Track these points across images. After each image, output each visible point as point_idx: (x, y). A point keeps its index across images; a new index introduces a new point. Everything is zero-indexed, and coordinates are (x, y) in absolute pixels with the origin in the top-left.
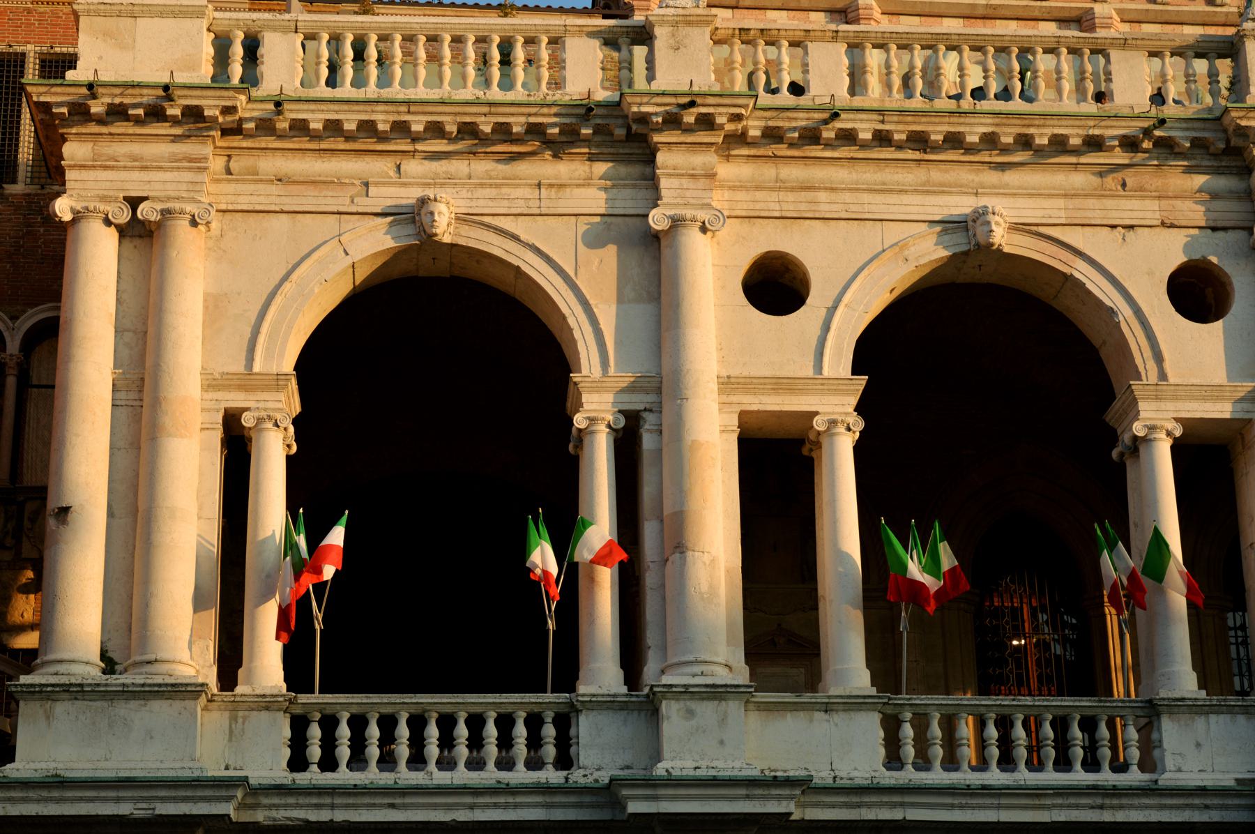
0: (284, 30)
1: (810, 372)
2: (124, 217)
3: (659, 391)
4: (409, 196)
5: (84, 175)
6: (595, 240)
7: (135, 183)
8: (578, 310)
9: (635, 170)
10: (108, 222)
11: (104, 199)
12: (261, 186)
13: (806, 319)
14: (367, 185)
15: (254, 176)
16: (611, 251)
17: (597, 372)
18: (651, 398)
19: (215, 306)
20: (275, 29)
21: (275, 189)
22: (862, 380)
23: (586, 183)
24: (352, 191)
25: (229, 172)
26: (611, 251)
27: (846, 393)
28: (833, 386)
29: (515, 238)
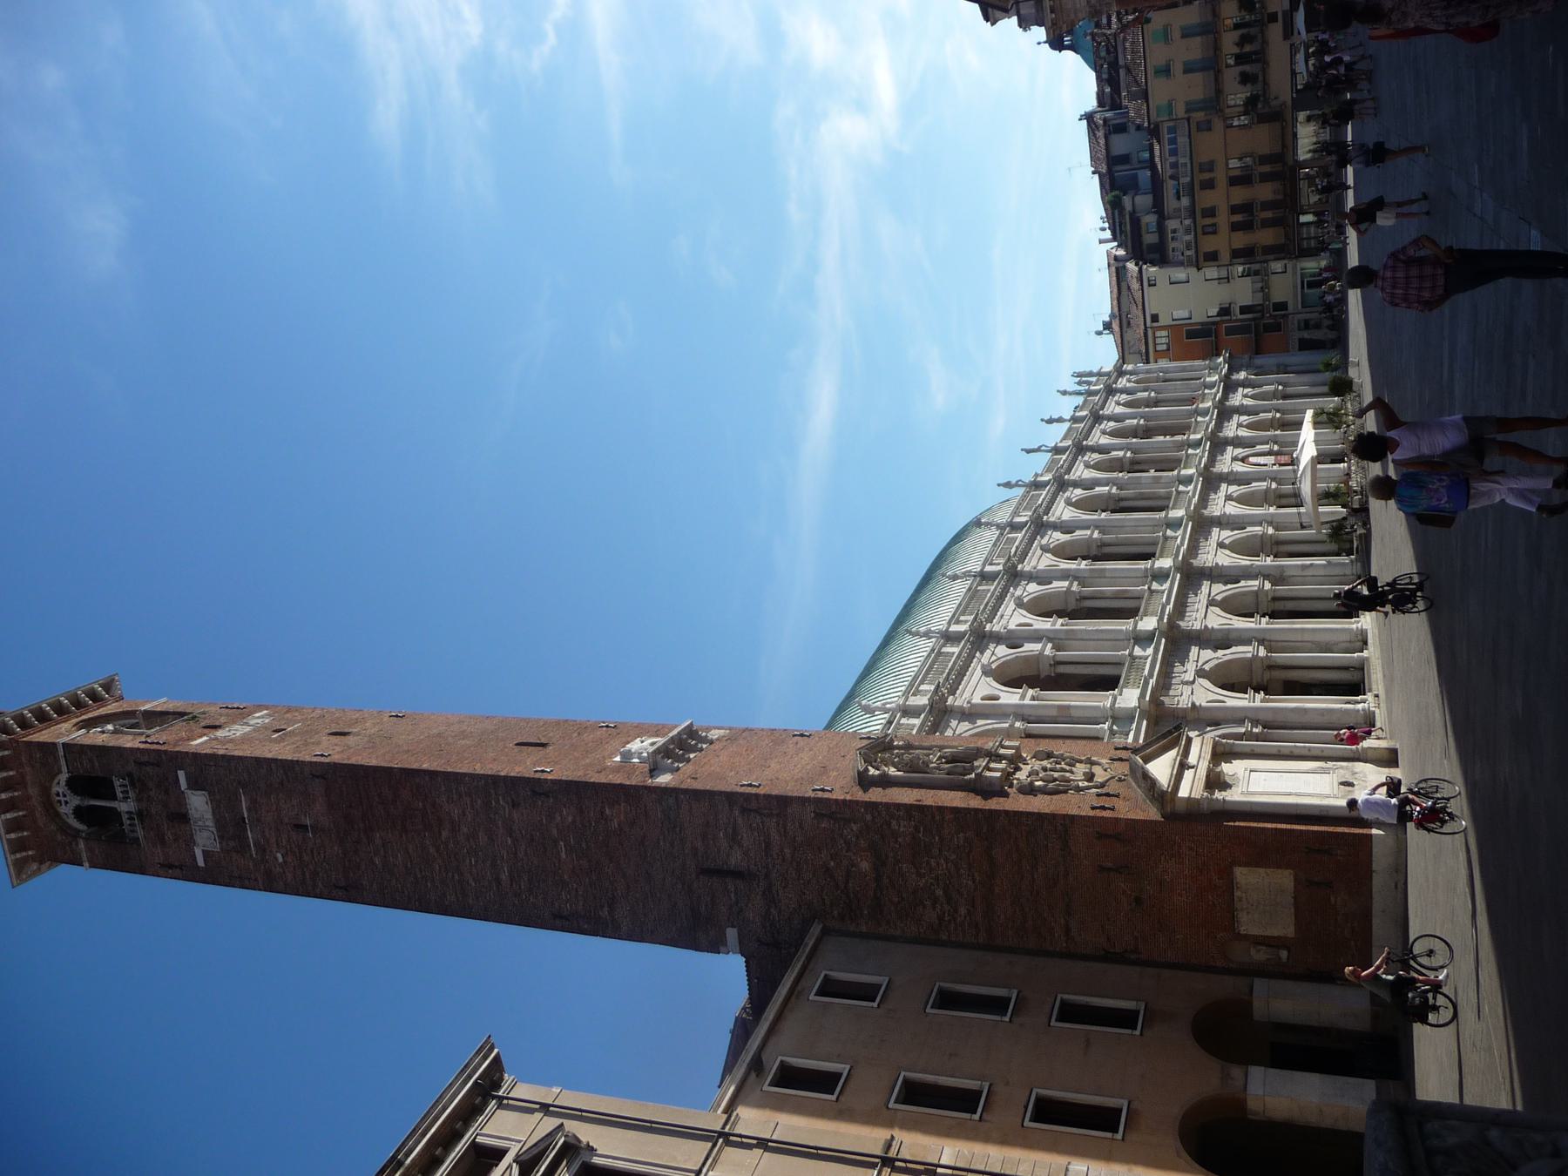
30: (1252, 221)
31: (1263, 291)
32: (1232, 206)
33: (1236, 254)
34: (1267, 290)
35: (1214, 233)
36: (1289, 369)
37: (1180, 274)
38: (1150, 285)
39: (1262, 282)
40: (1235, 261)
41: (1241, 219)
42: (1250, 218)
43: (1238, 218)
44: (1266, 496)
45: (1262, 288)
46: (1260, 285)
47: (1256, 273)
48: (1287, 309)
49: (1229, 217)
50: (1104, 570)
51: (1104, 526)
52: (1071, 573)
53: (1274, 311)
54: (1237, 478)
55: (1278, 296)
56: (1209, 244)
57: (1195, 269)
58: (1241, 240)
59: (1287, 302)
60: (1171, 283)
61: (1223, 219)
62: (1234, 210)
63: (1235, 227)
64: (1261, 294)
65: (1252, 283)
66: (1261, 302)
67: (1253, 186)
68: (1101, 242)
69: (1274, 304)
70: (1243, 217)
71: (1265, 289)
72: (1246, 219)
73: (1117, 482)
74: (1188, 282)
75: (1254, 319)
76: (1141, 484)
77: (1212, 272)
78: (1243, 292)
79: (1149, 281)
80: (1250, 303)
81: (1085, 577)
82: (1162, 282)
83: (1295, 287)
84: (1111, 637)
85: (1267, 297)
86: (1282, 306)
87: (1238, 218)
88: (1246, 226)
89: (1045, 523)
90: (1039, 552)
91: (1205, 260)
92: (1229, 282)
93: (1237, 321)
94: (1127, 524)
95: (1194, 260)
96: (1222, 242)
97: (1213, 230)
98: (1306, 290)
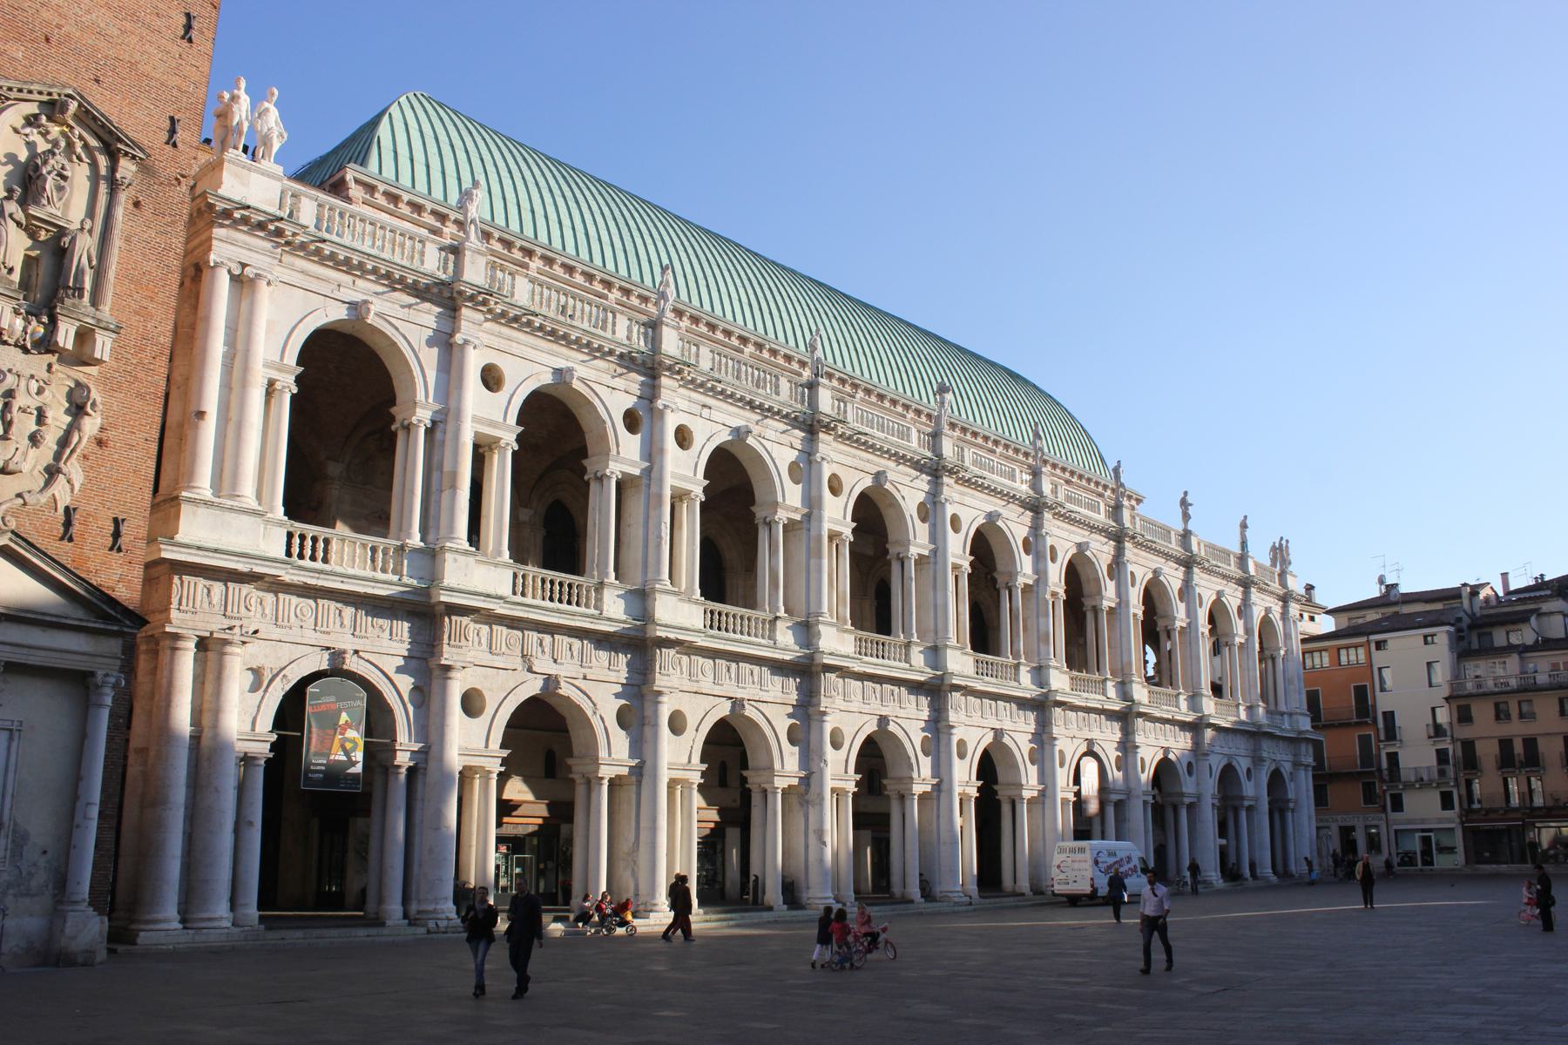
0: (311, 198)
1: (501, 420)
2: (237, 272)
3: (446, 415)
4: (358, 297)
5: (221, 244)
6: (430, 343)
7: (245, 256)
8: (418, 369)
9: (448, 312)
10: (229, 271)
11: (229, 259)
12: (293, 272)
13: (502, 396)
14: (339, 286)
15: (291, 268)
16: (436, 350)
17: (423, 399)
18: (443, 417)
19: (270, 323)
20: (306, 196)
21: (300, 276)
22: (521, 429)
23: (428, 312)
24: (333, 287)
25: (280, 261)
26: (436, 350)
27: (513, 432)
28: (508, 428)
29: (397, 329)
30: (1514, 766)
31: (1417, 781)
32: (1535, 739)
33: (1468, 746)
34: (1417, 786)
35: (1498, 718)
36: (1277, 817)
37: (1442, 674)
38: (1425, 637)
39: (1429, 780)
40: (1459, 745)
41: (1516, 752)
42: (1517, 764)
43: (1518, 748)
44: (1013, 785)
45: (1422, 779)
46: (1425, 778)
47: (1442, 773)
48: (1394, 810)
49: (1518, 736)
50: (819, 556)
51: (935, 563)
52: (815, 512)
53: (1391, 795)
54: (1046, 746)
55: (1409, 799)
56: (1483, 713)
57: (1447, 695)
58: (1488, 752)
59: (1402, 811)
60: (1429, 664)
61: (1516, 729)
62: (1530, 743)
63: (1505, 744)
64: (1413, 779)
65: (1428, 768)
66: (1403, 779)
67: (1563, 767)
68: (1505, 576)
69: (1400, 795)
70: (1519, 755)
71: (1422, 784)
72: (1517, 759)
73: (1041, 585)
74: (1430, 685)
75: (1380, 770)
76: (1038, 617)
77: (1443, 717)
78: (1417, 755)
79: (1433, 635)
80: (1401, 766)
81: (809, 530)
82: (1431, 653)
83: (1423, 821)
84: (651, 560)
85: (1409, 786)
86: (1398, 805)
87: (1518, 748)
88: (1506, 759)
89: (939, 481)
90: (874, 469)
91: (1459, 707)
92: (1430, 737)
93: (1378, 749)
94: (940, 595)
95: (1460, 693)
96: (1485, 729)
97: (1501, 714)
98: (1418, 835)
